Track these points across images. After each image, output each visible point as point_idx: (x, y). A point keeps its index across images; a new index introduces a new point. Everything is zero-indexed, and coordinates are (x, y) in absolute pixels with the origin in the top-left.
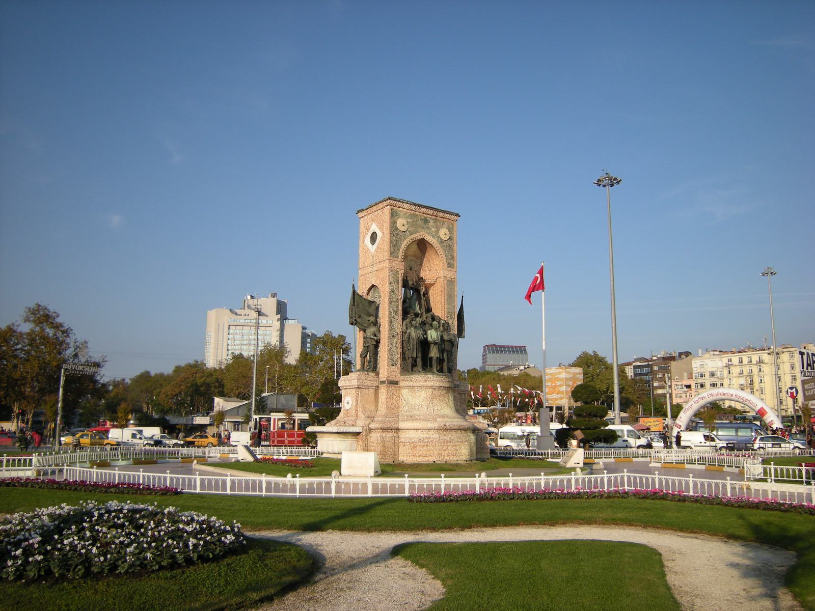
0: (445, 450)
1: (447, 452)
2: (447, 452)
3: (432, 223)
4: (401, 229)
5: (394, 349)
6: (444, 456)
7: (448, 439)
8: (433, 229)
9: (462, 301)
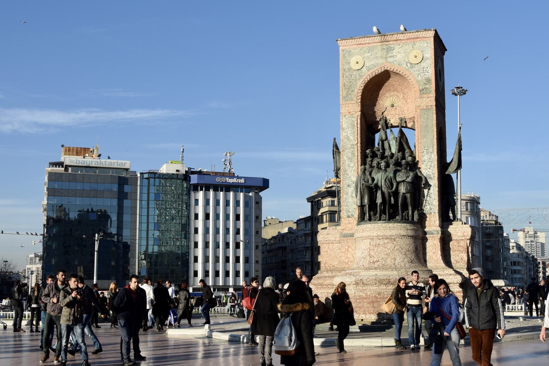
0: (360, 307)
1: (362, 310)
2: (362, 310)
4: (354, 68)
5: (350, 200)
7: (364, 295)
8: (399, 55)
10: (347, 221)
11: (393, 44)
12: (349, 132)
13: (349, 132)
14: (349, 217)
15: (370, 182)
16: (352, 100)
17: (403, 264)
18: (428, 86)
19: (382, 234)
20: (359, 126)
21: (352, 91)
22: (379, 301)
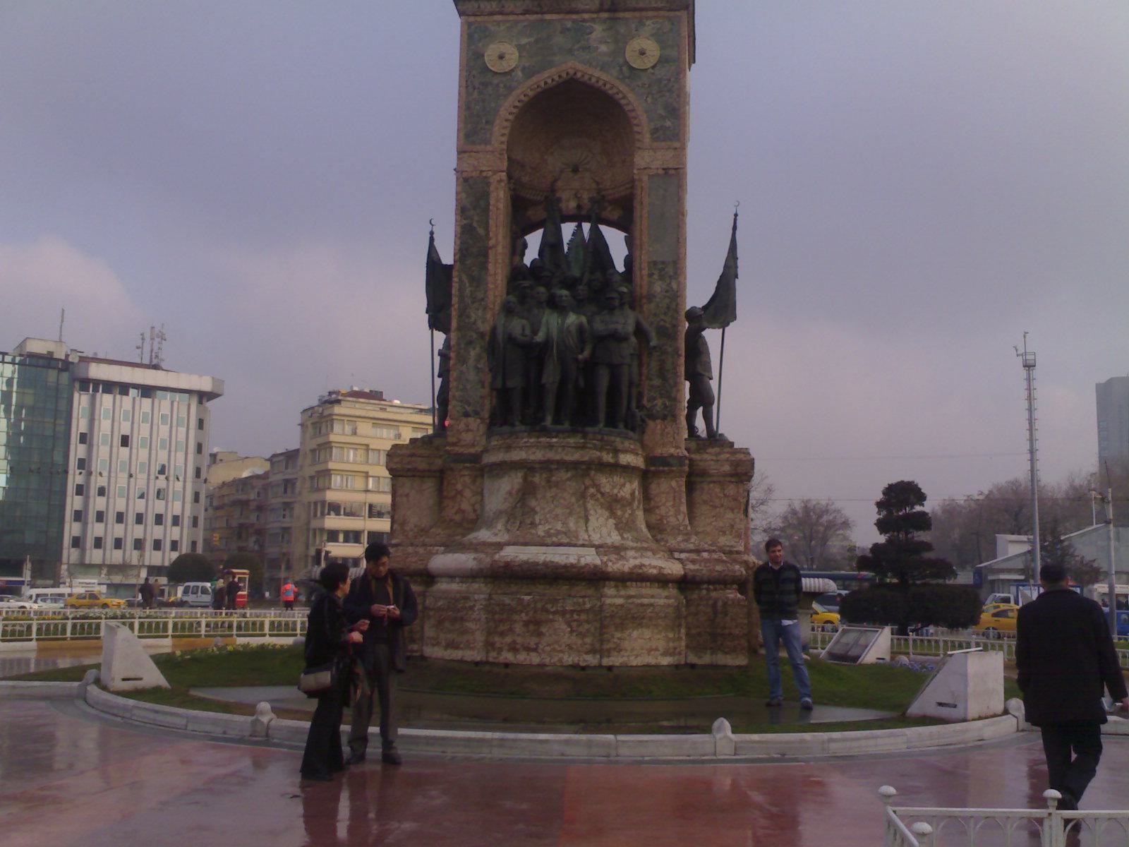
1: (508, 639)
3: (598, 31)
5: (472, 376)
6: (500, 650)
7: (514, 603)
8: (603, 48)
9: (735, 228)
10: (462, 426)
11: (593, 20)
12: (476, 218)
13: (476, 218)
14: (466, 415)
15: (528, 332)
16: (487, 142)
17: (604, 531)
18: (668, 123)
19: (558, 457)
20: (501, 206)
21: (487, 122)
22: (552, 621)
